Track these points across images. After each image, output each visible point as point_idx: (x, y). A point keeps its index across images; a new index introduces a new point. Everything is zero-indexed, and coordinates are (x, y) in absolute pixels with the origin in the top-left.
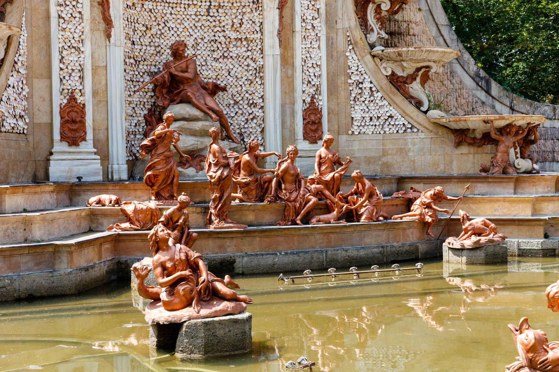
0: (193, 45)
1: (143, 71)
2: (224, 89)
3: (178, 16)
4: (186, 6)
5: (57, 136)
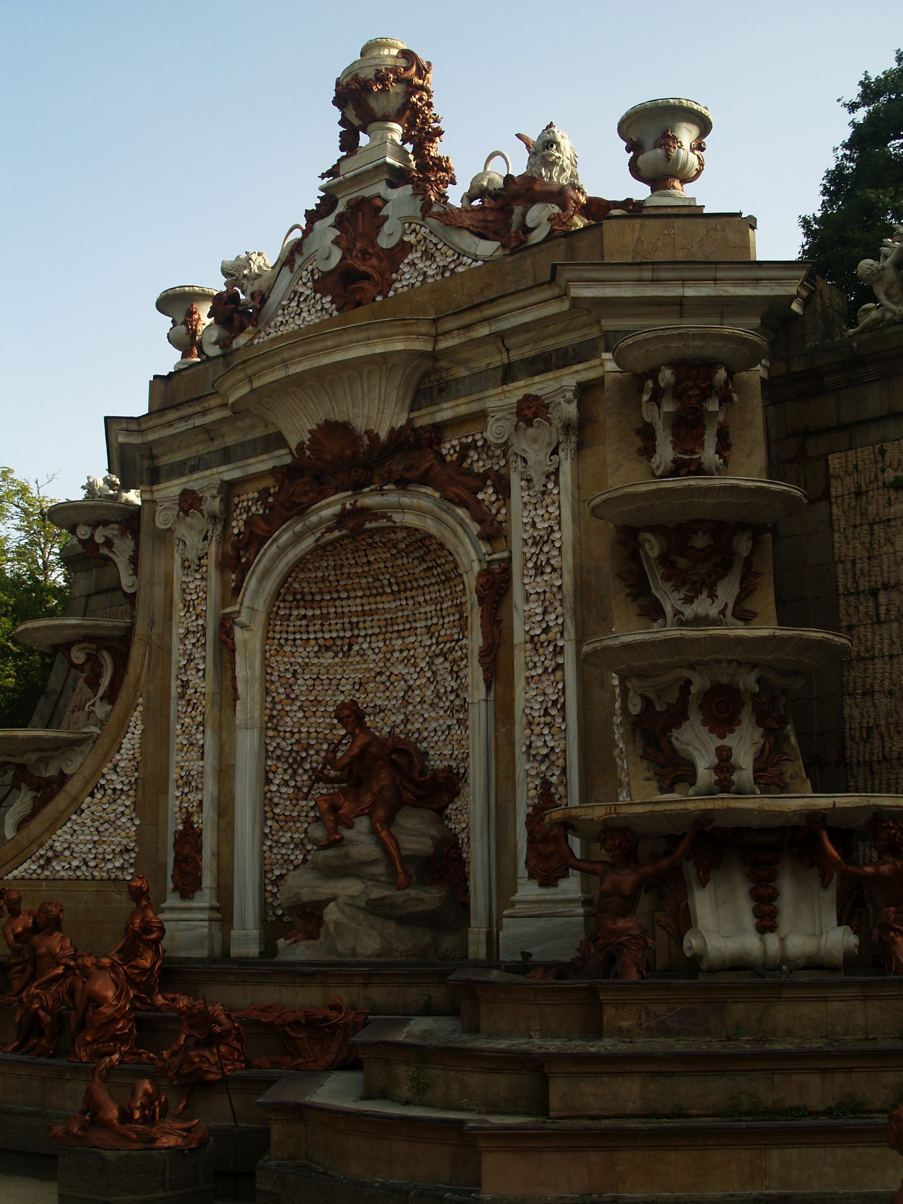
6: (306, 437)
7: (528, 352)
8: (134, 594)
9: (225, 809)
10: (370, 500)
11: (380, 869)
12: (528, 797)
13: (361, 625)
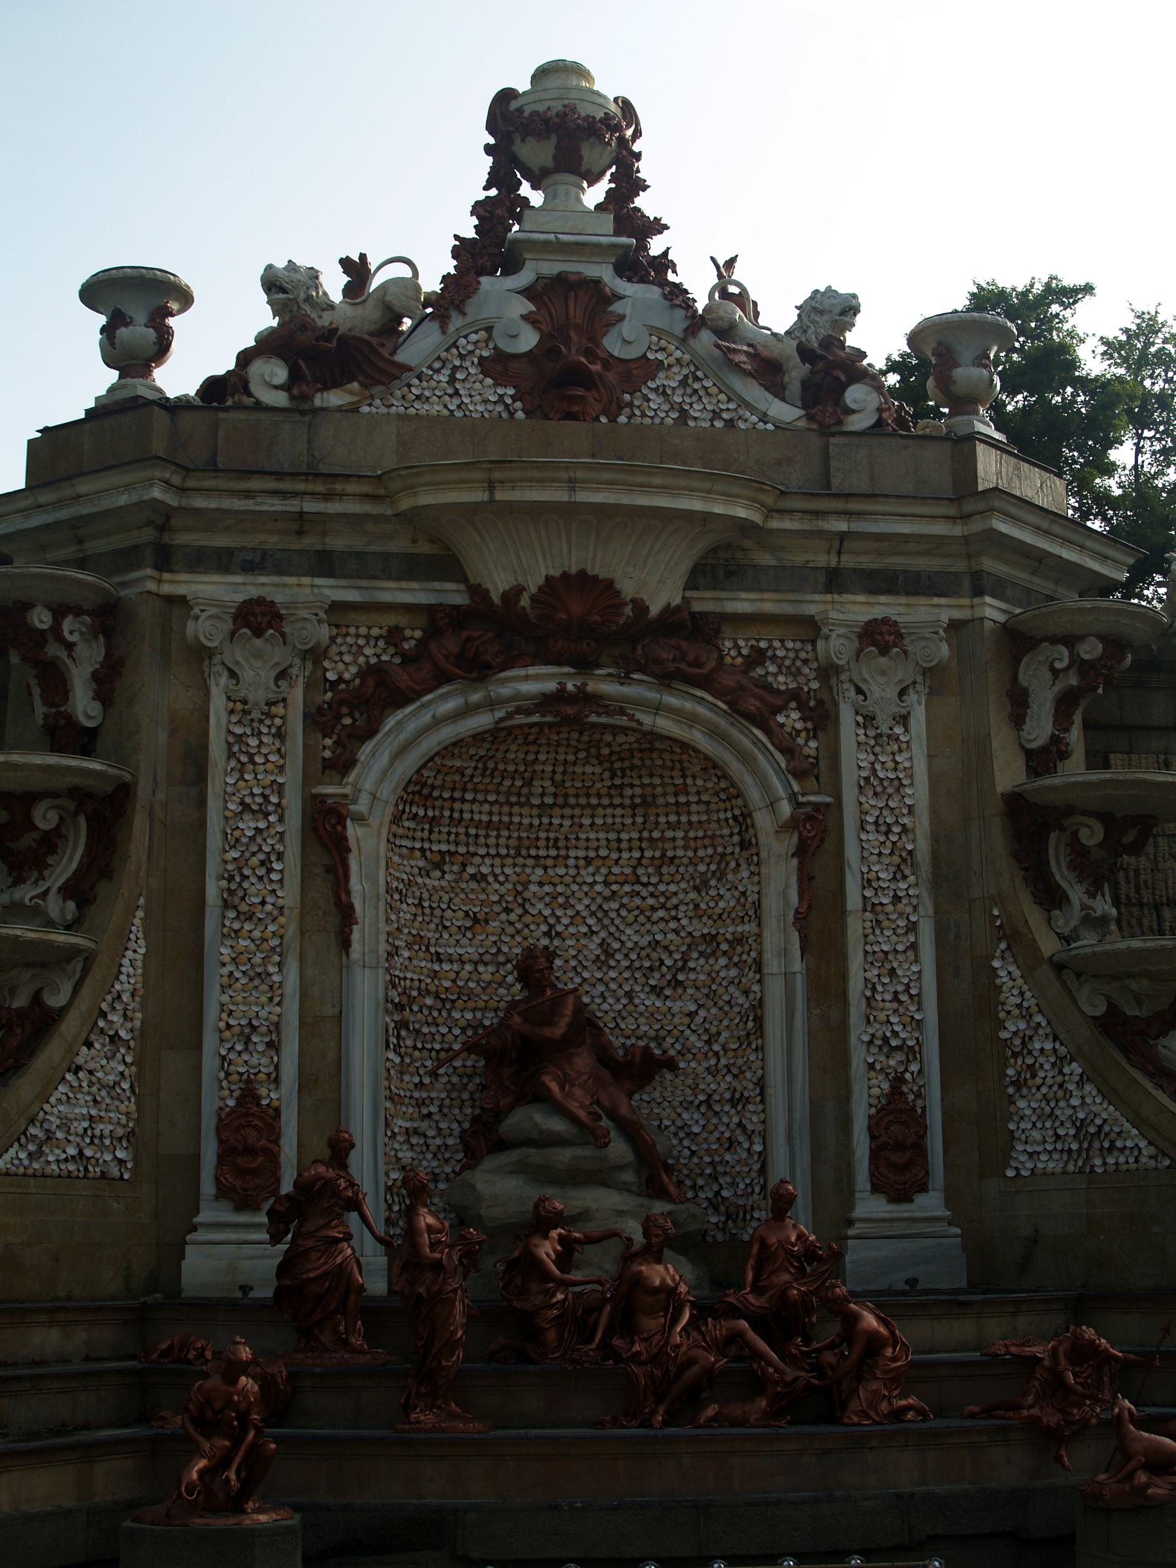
0: (598, 956)
1: (462, 1023)
3: (560, 889)
4: (582, 863)
5: (208, 1187)
6: (534, 583)
7: (867, 562)
8: (92, 733)
10: (603, 685)
11: (628, 1176)
12: (870, 1096)
13: (482, 840)
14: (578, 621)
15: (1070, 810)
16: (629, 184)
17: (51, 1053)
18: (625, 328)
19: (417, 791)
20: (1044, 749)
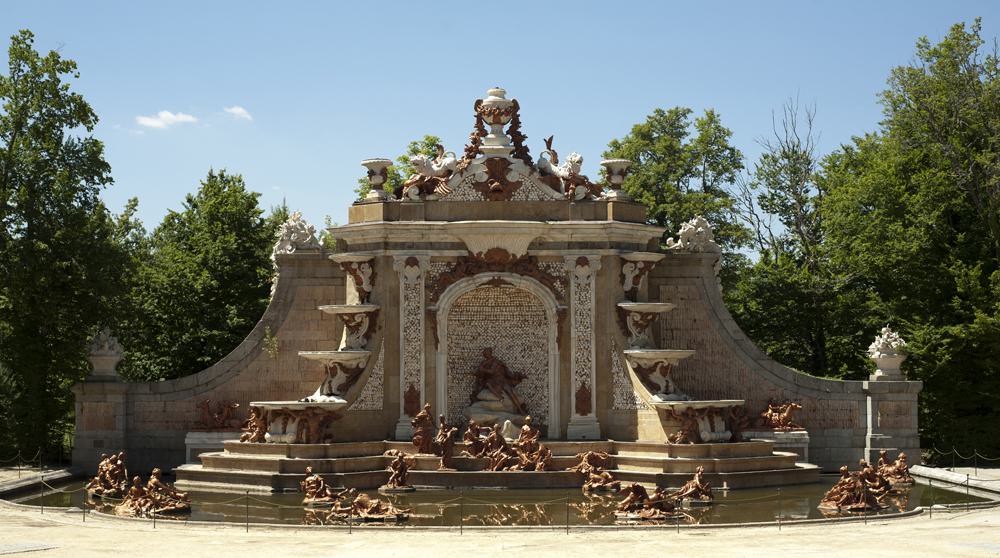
2: (526, 377)
5: (402, 411)
6: (485, 251)
8: (369, 293)
9: (431, 384)
14: (498, 261)
15: (631, 312)
16: (516, 123)
17: (360, 380)
18: (513, 173)
19: (456, 305)
20: (630, 291)
